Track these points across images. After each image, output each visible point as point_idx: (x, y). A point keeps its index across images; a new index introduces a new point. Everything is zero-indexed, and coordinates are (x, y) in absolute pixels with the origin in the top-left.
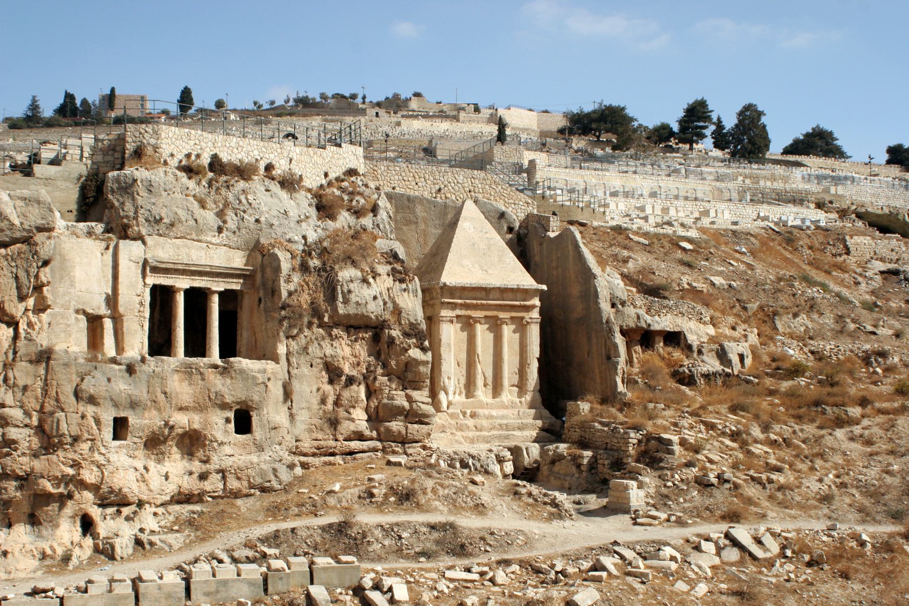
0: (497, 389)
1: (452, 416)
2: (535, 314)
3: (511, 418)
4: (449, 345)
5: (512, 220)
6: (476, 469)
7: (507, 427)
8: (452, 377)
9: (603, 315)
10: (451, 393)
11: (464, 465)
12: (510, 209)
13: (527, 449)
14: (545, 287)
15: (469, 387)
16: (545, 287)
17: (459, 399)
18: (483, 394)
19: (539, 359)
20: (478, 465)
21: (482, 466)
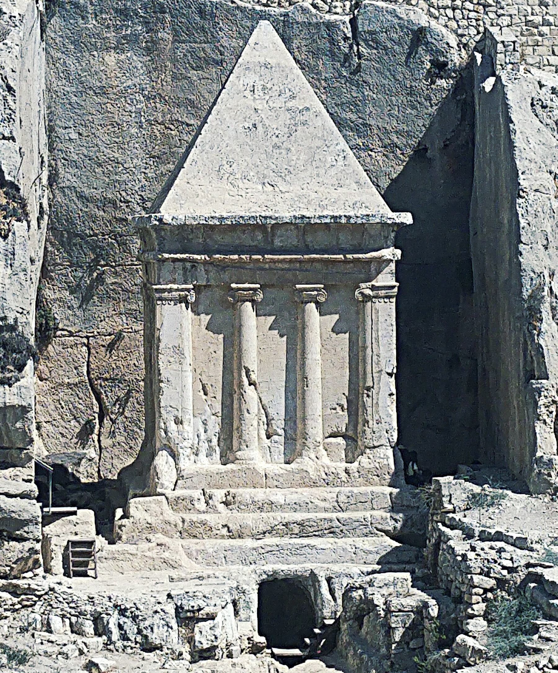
0: (294, 441)
1: (175, 503)
2: (386, 279)
3: (317, 509)
4: (178, 350)
5: (441, 46)
6: (124, 637)
7: (304, 529)
8: (188, 417)
9: (526, 282)
10: (184, 453)
11: (101, 629)
12: (443, 20)
13: (329, 580)
14: (407, 218)
15: (229, 440)
16: (407, 218)
17: (210, 464)
18: (259, 454)
19: (399, 376)
20: (130, 628)
21: (139, 632)
